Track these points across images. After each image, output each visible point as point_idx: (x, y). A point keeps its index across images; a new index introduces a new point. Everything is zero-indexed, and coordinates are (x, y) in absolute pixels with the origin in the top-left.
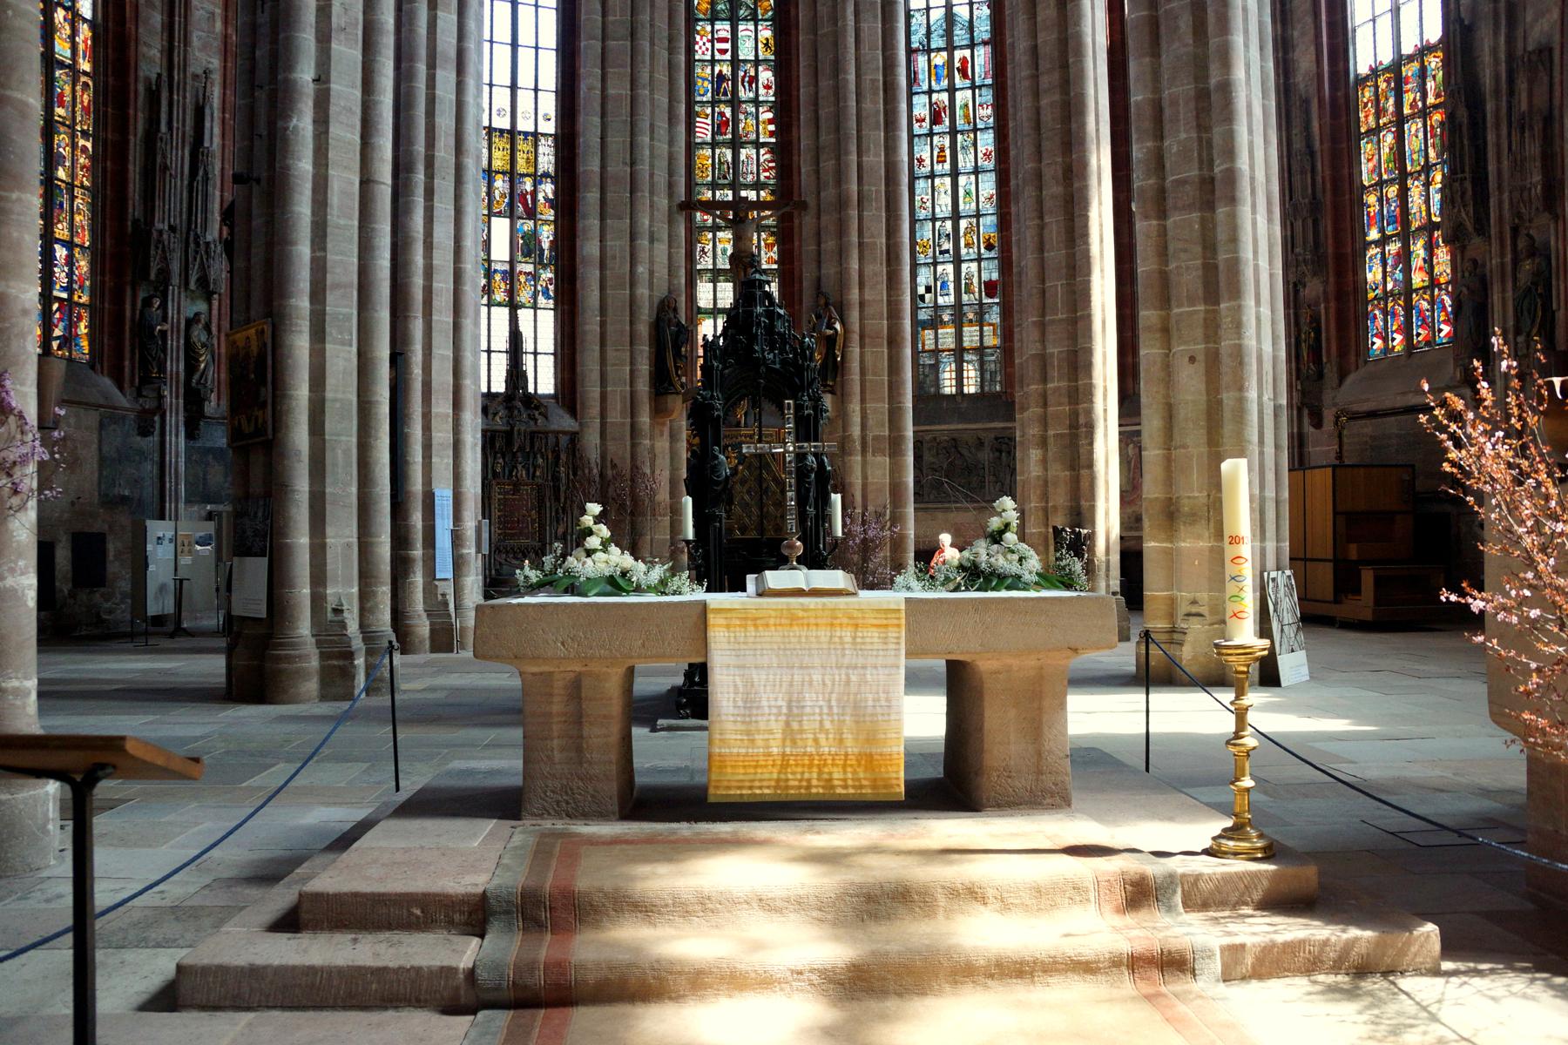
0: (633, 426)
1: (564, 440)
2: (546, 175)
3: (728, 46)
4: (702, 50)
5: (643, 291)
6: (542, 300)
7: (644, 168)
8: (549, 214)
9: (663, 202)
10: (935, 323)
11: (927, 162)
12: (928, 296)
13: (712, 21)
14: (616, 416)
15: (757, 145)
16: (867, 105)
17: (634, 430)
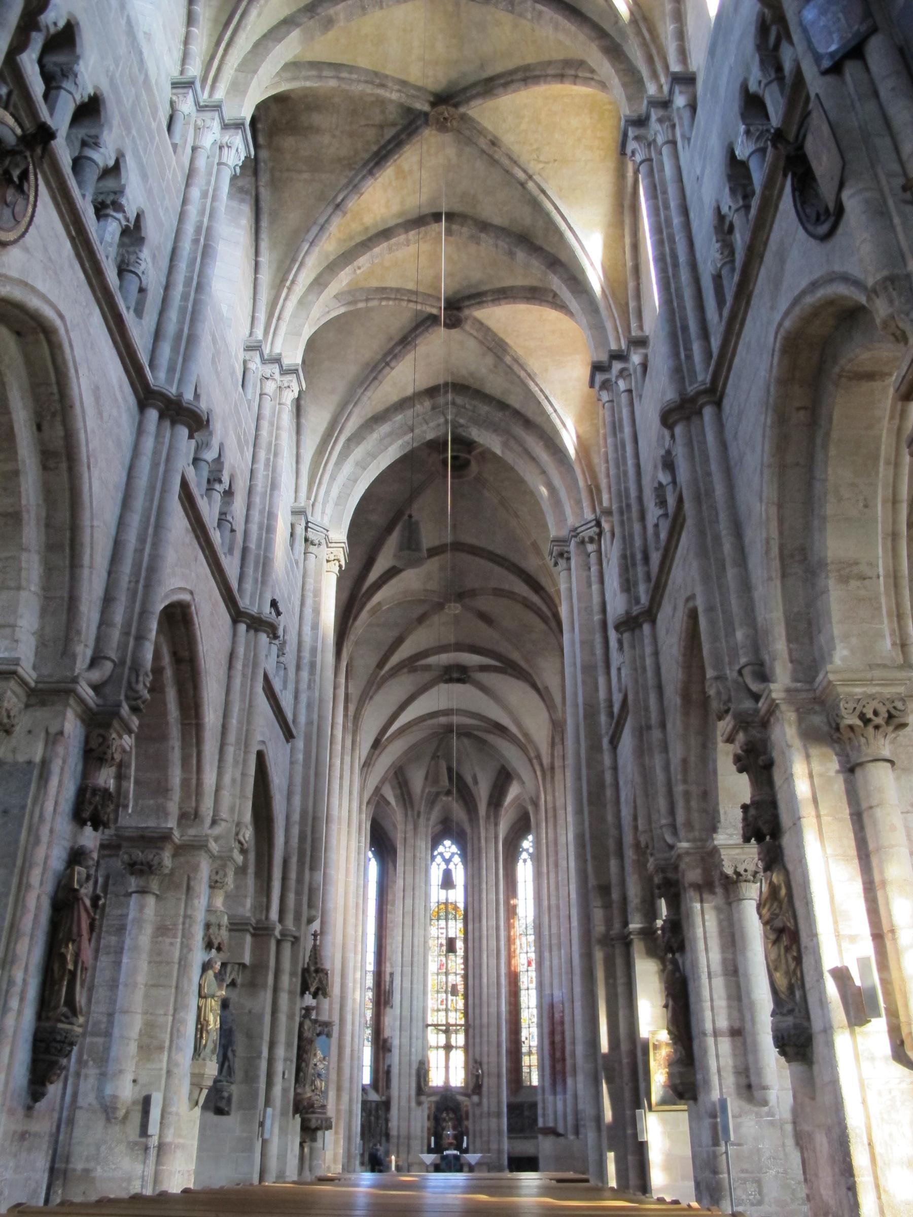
0: (409, 1108)
1: (374, 1105)
2: (369, 988)
3: (444, 931)
4: (433, 931)
5: (413, 1058)
6: (366, 1042)
7: (414, 1014)
8: (370, 1005)
9: (421, 1024)
10: (530, 1053)
11: (526, 983)
12: (526, 1042)
13: (438, 920)
14: (404, 1103)
15: (456, 974)
16: (491, 991)
17: (409, 1108)
